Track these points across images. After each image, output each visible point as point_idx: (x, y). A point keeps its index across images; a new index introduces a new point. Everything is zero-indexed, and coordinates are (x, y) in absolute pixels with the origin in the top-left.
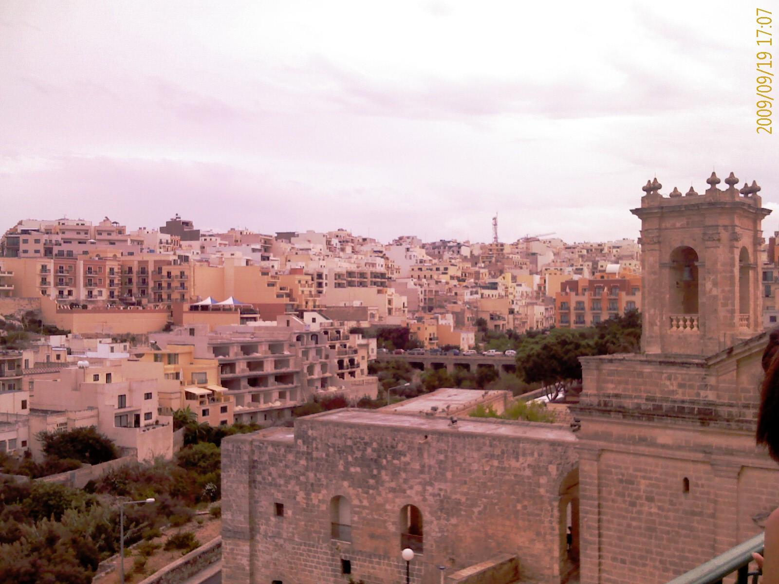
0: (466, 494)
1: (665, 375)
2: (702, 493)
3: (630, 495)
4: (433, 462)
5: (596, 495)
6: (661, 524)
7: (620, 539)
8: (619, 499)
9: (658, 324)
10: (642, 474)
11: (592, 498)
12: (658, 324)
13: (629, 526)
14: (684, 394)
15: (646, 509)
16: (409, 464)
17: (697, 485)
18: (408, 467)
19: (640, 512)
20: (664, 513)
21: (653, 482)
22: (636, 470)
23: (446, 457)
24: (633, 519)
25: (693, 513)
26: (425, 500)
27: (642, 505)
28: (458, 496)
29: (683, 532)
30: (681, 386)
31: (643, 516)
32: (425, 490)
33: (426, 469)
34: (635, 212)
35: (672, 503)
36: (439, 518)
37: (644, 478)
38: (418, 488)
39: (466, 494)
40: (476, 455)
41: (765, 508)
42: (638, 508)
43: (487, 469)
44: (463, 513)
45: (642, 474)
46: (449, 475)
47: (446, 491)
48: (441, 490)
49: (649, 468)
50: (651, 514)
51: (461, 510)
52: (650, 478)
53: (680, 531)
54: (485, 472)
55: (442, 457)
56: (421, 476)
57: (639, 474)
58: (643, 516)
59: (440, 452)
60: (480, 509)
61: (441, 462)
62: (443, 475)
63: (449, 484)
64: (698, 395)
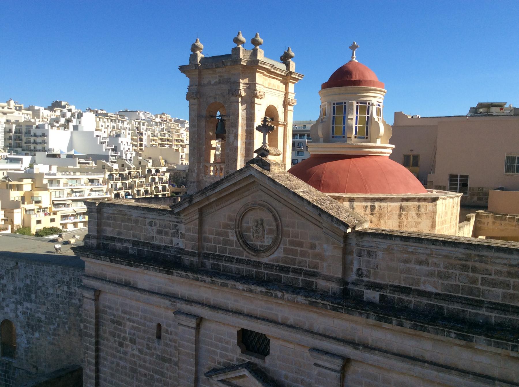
0: (44, 313)
1: (148, 221)
2: (171, 340)
3: (119, 336)
4: (22, 285)
5: (93, 333)
6: (140, 366)
7: (112, 375)
8: (112, 339)
9: (196, 171)
10: (128, 317)
11: (90, 336)
12: (196, 171)
13: (118, 365)
14: (161, 240)
15: (129, 349)
16: (6, 285)
17: (167, 332)
18: (5, 288)
19: (125, 353)
20: (143, 356)
21: (135, 325)
22: (123, 312)
23: (31, 281)
24: (121, 359)
25: (164, 360)
26: (17, 316)
27: (127, 346)
28: (40, 315)
29: (156, 376)
30: (159, 232)
31: (128, 357)
32: (17, 309)
33: (18, 291)
34: (182, 69)
35: (149, 348)
36: (26, 332)
37: (129, 320)
38: (12, 306)
39: (44, 313)
40: (51, 280)
41: (219, 363)
42: (124, 348)
43: (59, 292)
44: (43, 329)
45: (128, 317)
46: (33, 296)
47: (31, 309)
48: (27, 308)
49: (133, 311)
50: (133, 355)
51: (42, 326)
52: (133, 321)
53: (154, 375)
54: (58, 296)
55: (28, 281)
56: (14, 296)
57: (125, 315)
58: (128, 357)
59: (26, 277)
60: (55, 327)
61: (27, 285)
62: (29, 296)
63: (33, 304)
64: (172, 242)
